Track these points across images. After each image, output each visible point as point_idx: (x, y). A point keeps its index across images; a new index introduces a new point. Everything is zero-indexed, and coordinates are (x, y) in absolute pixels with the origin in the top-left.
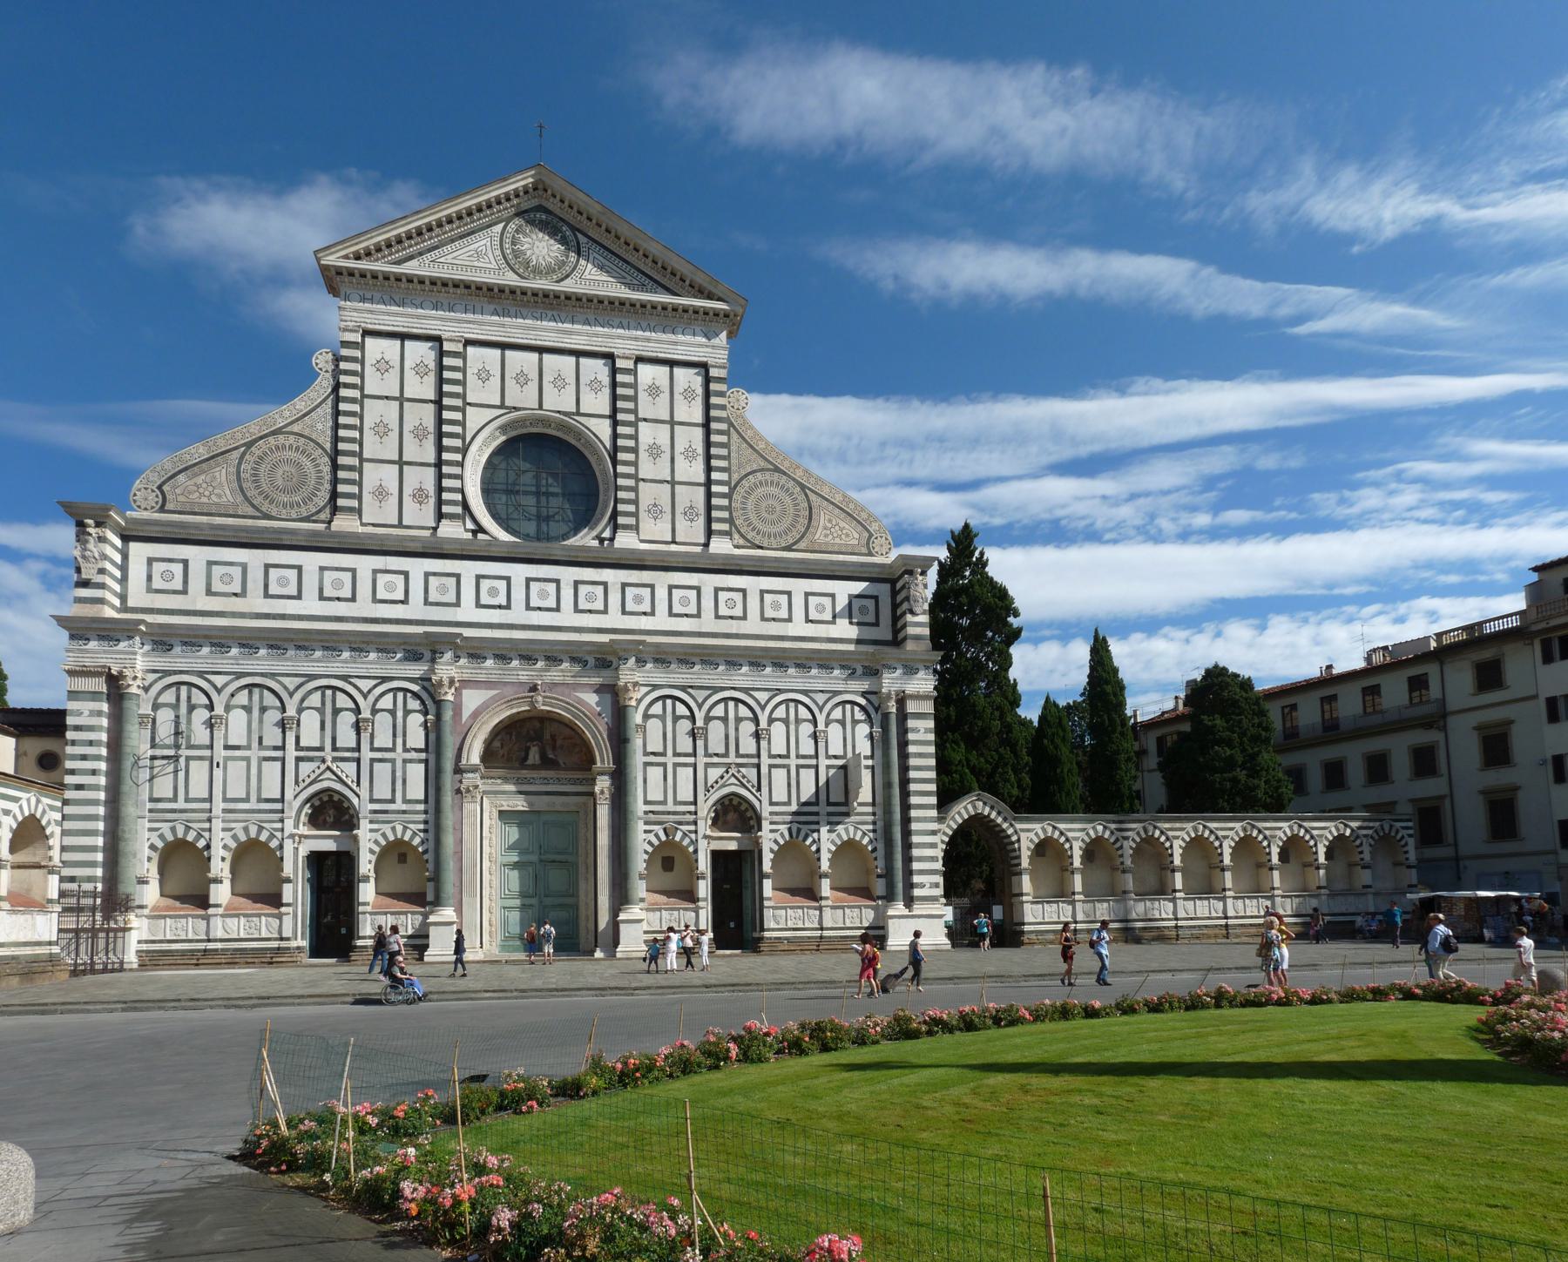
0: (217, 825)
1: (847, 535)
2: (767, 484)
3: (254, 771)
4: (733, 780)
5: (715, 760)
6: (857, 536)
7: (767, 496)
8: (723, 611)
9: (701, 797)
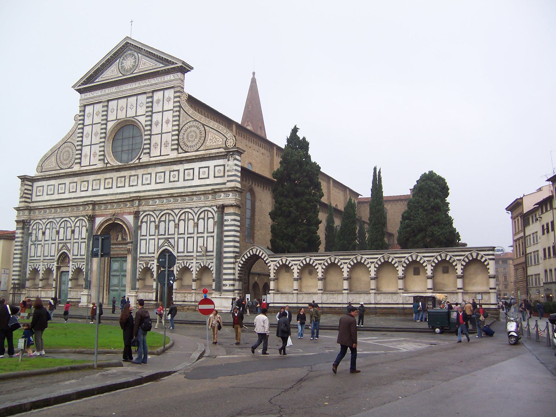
0: (41, 264)
1: (218, 141)
2: (191, 127)
3: (50, 247)
4: (166, 244)
6: (221, 140)
7: (191, 132)
8: (172, 179)
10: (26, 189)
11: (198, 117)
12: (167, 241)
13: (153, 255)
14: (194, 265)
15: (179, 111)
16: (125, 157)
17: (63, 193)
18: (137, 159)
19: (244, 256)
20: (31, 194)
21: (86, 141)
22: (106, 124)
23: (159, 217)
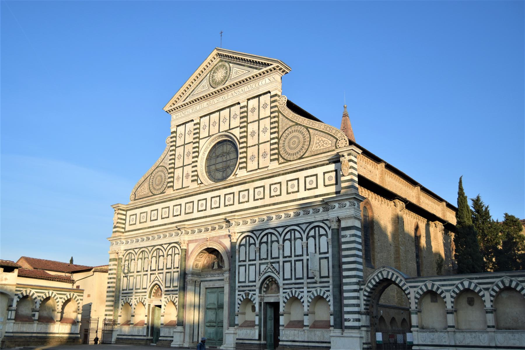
2: (293, 132)
5: (263, 261)
6: (330, 142)
9: (257, 279)
10: (119, 218)
11: (300, 120)
12: (271, 266)
13: (254, 284)
14: (305, 294)
15: (278, 117)
16: (219, 175)
17: (155, 220)
18: (233, 176)
19: (370, 282)
20: (124, 224)
21: (179, 163)
22: (198, 142)
23: (260, 238)
